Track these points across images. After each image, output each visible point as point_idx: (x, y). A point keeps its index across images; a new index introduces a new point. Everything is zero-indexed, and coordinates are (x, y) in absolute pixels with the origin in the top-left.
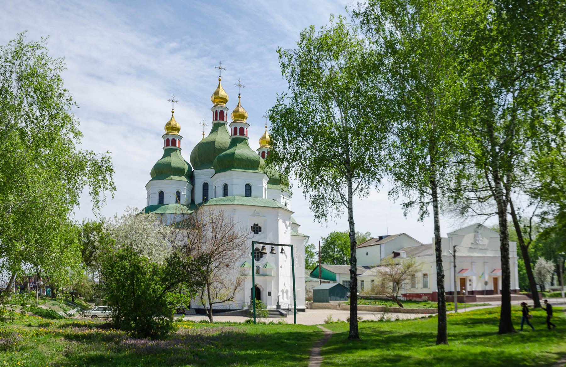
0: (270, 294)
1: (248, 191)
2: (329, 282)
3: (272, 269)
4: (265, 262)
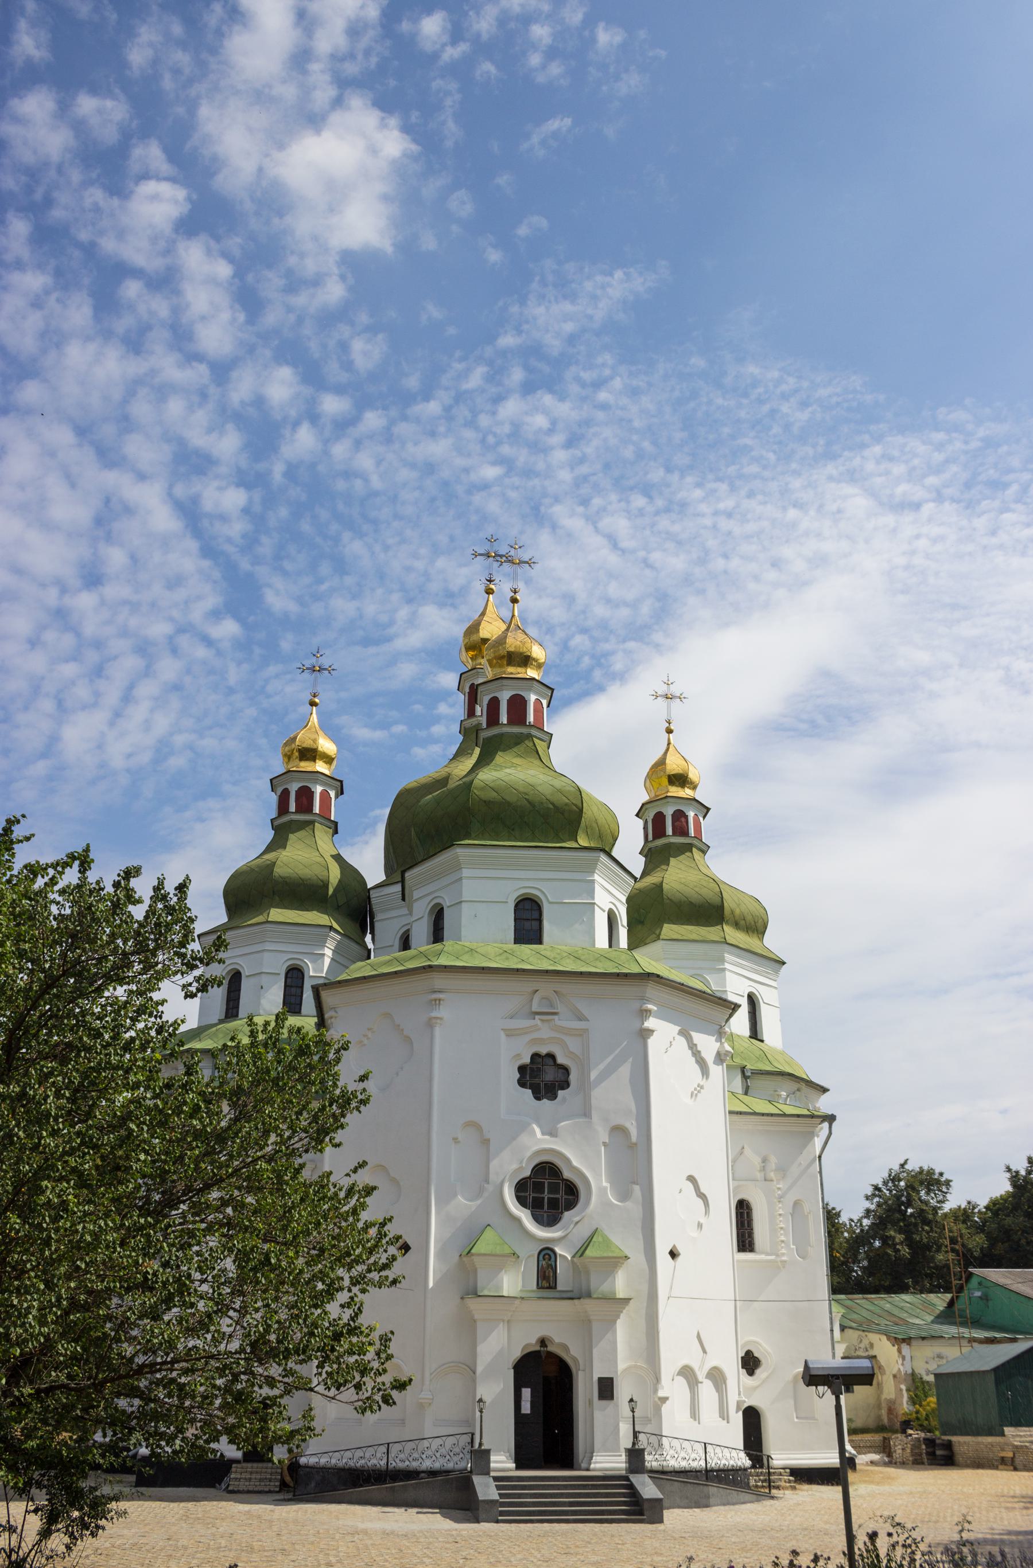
0: (606, 1388)
2: (1014, 1340)
3: (620, 1260)
4: (581, 1232)
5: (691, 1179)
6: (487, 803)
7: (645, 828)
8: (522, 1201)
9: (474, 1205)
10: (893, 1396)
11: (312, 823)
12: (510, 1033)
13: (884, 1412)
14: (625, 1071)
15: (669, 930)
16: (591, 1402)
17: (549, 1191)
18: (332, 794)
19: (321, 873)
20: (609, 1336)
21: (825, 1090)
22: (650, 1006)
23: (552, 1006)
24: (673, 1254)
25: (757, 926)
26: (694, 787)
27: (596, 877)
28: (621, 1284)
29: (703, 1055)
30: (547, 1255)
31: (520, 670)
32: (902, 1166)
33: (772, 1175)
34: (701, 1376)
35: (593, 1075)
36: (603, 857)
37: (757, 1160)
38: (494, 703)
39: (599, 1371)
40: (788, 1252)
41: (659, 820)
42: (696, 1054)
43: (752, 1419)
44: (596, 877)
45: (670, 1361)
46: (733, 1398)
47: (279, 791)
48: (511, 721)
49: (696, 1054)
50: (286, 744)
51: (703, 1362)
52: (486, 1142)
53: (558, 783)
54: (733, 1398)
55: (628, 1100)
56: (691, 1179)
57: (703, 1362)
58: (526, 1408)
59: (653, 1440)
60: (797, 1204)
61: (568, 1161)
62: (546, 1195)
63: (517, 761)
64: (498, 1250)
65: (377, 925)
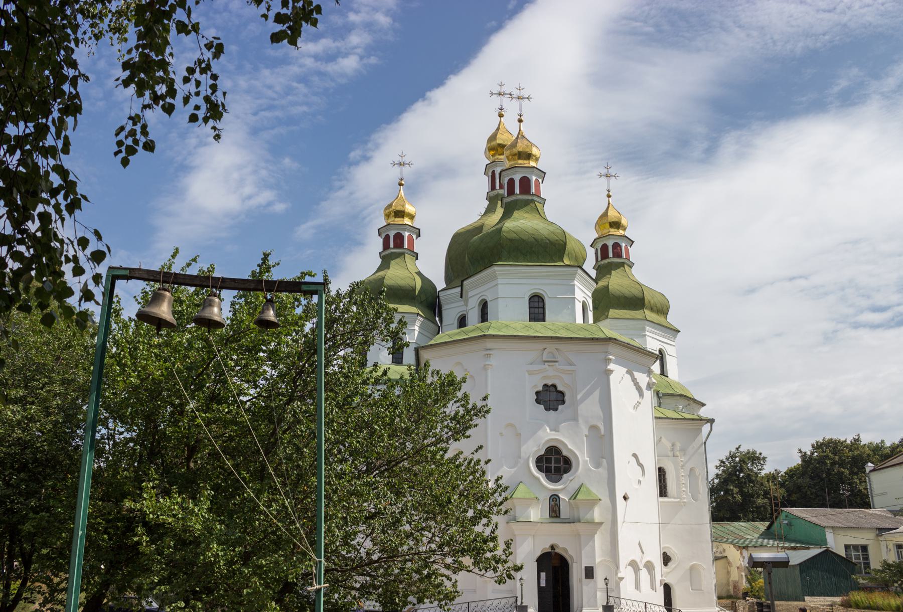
0: (589, 573)
1: (537, 308)
2: (808, 548)
4: (574, 486)
5: (635, 455)
6: (511, 240)
7: (596, 253)
8: (539, 468)
9: (513, 470)
10: (737, 579)
11: (404, 254)
12: (531, 373)
13: (731, 588)
14: (597, 394)
15: (613, 312)
16: (580, 581)
17: (554, 463)
18: (414, 237)
19: (412, 283)
20: (591, 543)
21: (703, 405)
22: (611, 357)
23: (554, 357)
24: (625, 498)
25: (662, 310)
26: (625, 229)
27: (576, 282)
28: (597, 514)
29: (640, 384)
30: (554, 500)
31: (525, 162)
32: (737, 449)
33: (678, 453)
34: (641, 566)
35: (579, 397)
36: (579, 271)
37: (668, 445)
38: (511, 182)
39: (585, 563)
40: (687, 497)
41: (605, 248)
42: (636, 384)
43: (667, 589)
44: (576, 282)
45: (625, 556)
46: (658, 578)
47: (383, 236)
48: (522, 192)
49: (636, 384)
50: (386, 209)
51: (642, 558)
52: (519, 435)
53: (551, 228)
54: (658, 578)
55: (598, 411)
56: (635, 455)
57: (642, 558)
58: (543, 584)
59: (617, 600)
60: (692, 470)
61: (566, 445)
62: (553, 465)
63: (526, 215)
64: (528, 496)
65: (444, 313)
